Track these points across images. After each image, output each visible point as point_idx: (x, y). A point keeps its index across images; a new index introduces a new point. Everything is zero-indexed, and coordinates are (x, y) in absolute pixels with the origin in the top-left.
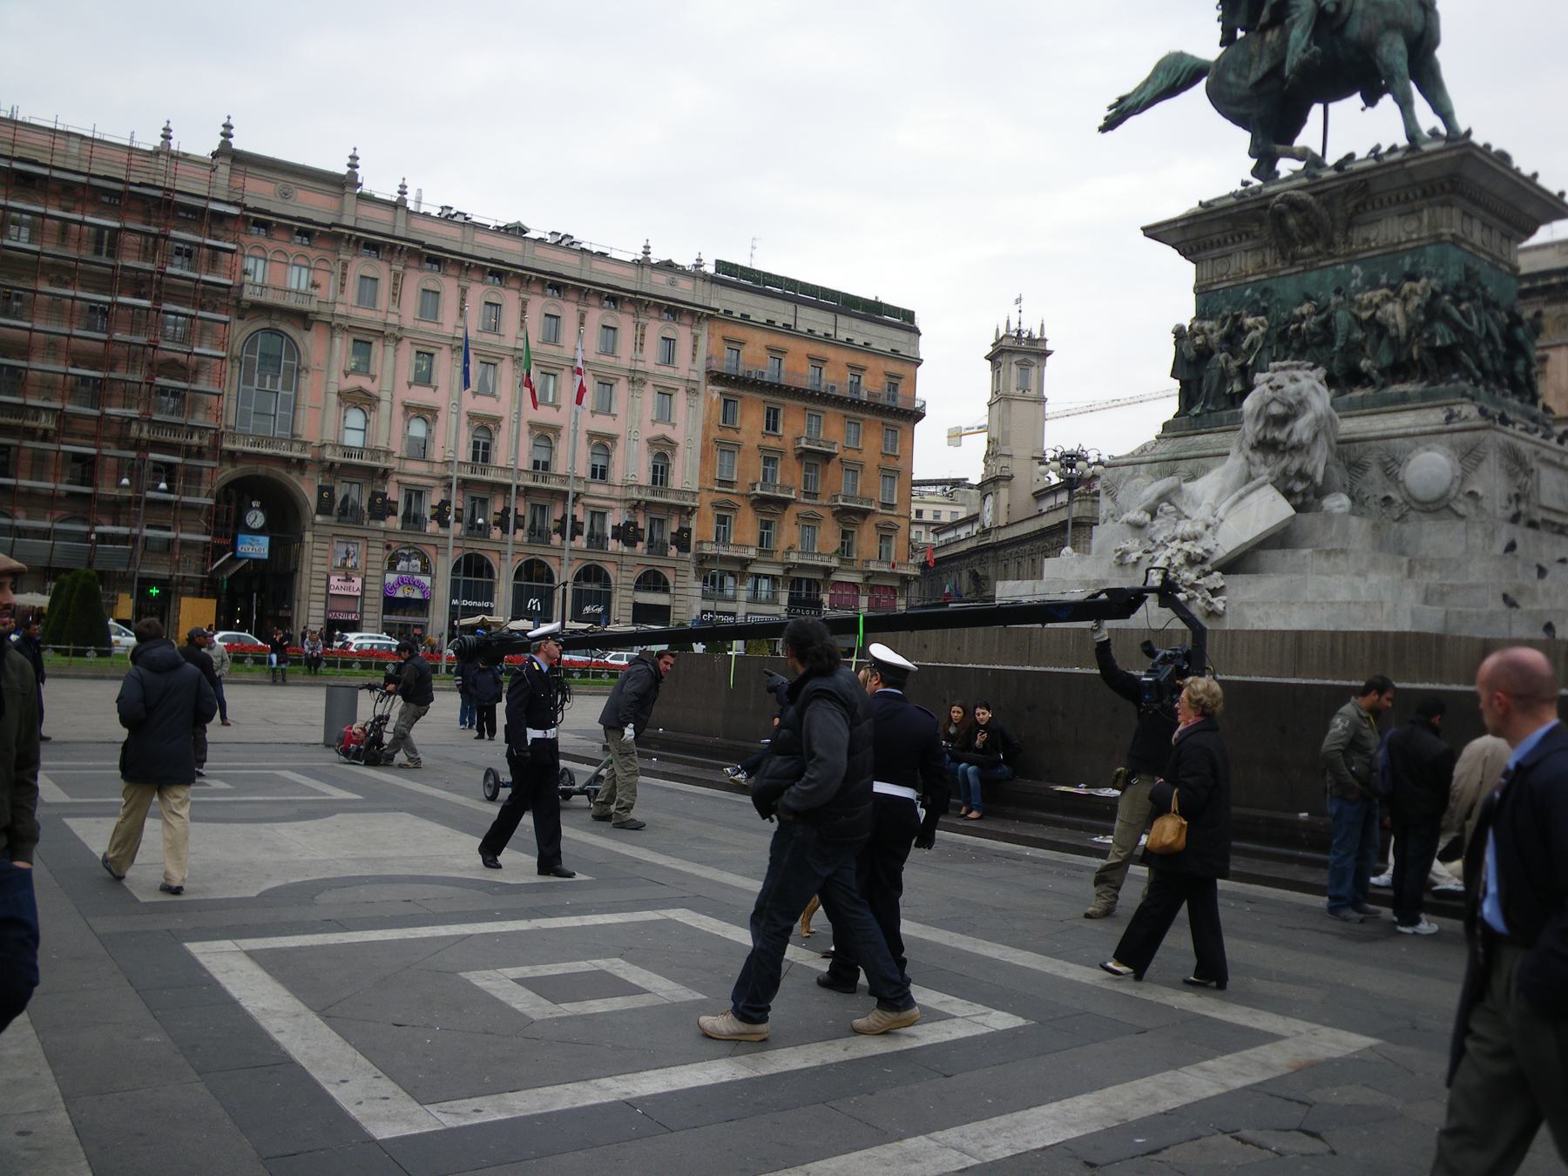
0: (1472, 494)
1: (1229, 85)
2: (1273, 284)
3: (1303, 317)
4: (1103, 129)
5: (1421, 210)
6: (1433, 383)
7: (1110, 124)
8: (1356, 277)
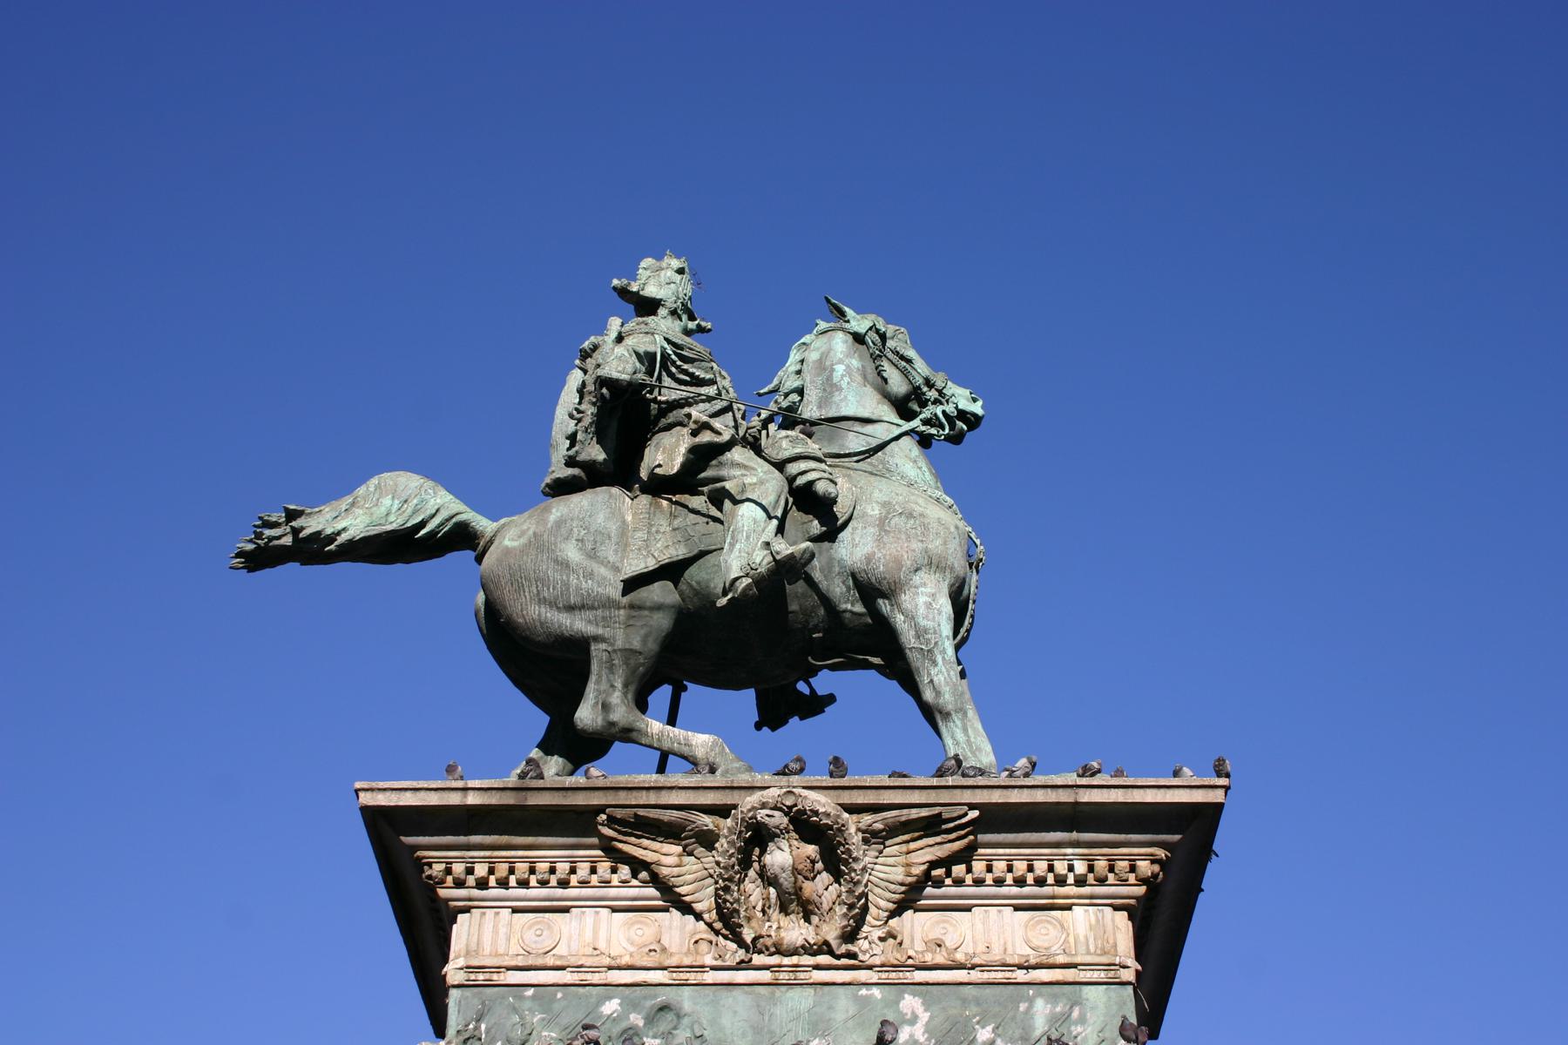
1: (565, 565)
2: (686, 999)
5: (1069, 908)
7: (260, 558)
8: (913, 1020)
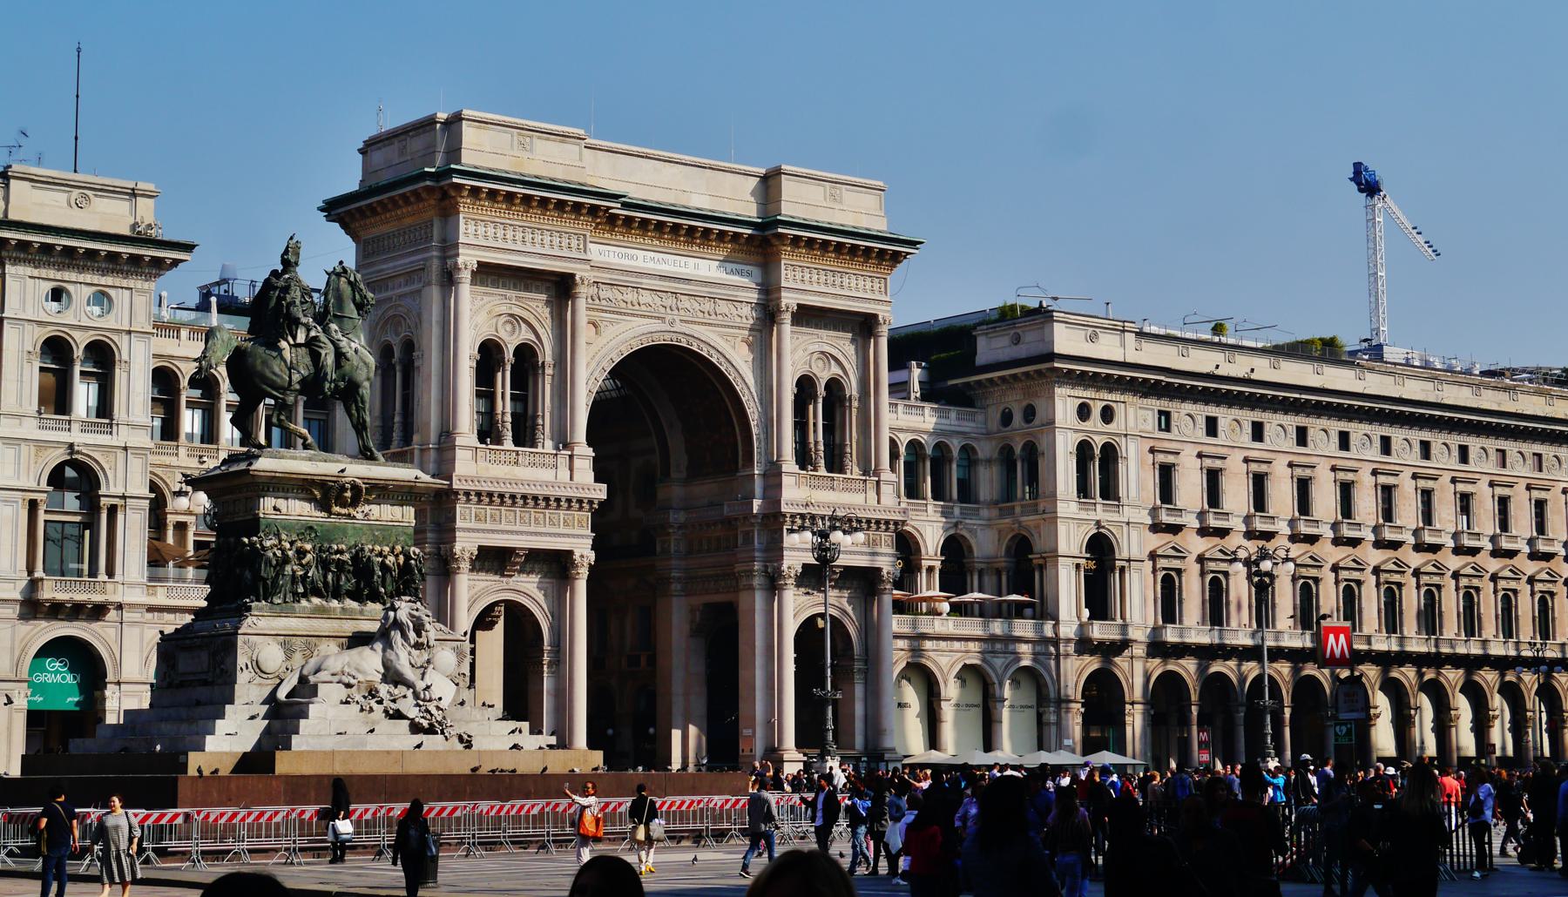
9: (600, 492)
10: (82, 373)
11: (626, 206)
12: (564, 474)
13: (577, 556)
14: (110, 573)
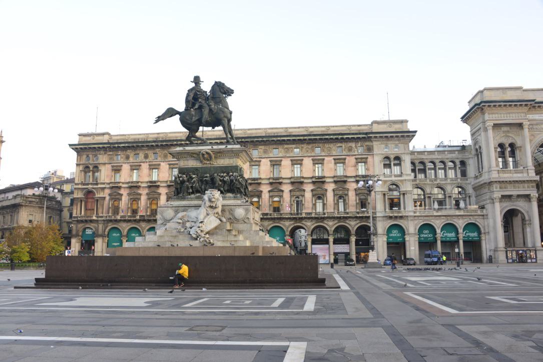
0: (248, 218)
1: (187, 119)
3: (206, 177)
4: (155, 123)
6: (236, 195)
7: (157, 121)
9: (538, 178)
10: (394, 164)
11: (536, 103)
12: (525, 175)
13: (532, 195)
14: (405, 209)
